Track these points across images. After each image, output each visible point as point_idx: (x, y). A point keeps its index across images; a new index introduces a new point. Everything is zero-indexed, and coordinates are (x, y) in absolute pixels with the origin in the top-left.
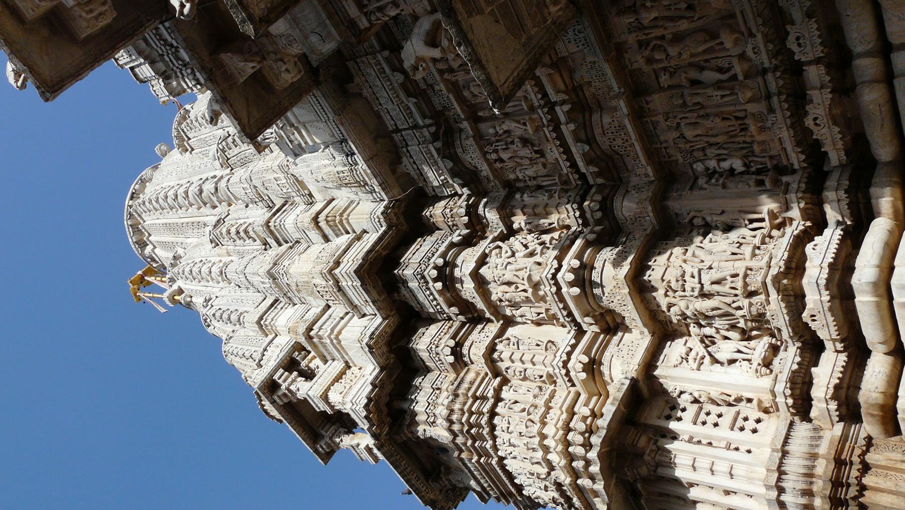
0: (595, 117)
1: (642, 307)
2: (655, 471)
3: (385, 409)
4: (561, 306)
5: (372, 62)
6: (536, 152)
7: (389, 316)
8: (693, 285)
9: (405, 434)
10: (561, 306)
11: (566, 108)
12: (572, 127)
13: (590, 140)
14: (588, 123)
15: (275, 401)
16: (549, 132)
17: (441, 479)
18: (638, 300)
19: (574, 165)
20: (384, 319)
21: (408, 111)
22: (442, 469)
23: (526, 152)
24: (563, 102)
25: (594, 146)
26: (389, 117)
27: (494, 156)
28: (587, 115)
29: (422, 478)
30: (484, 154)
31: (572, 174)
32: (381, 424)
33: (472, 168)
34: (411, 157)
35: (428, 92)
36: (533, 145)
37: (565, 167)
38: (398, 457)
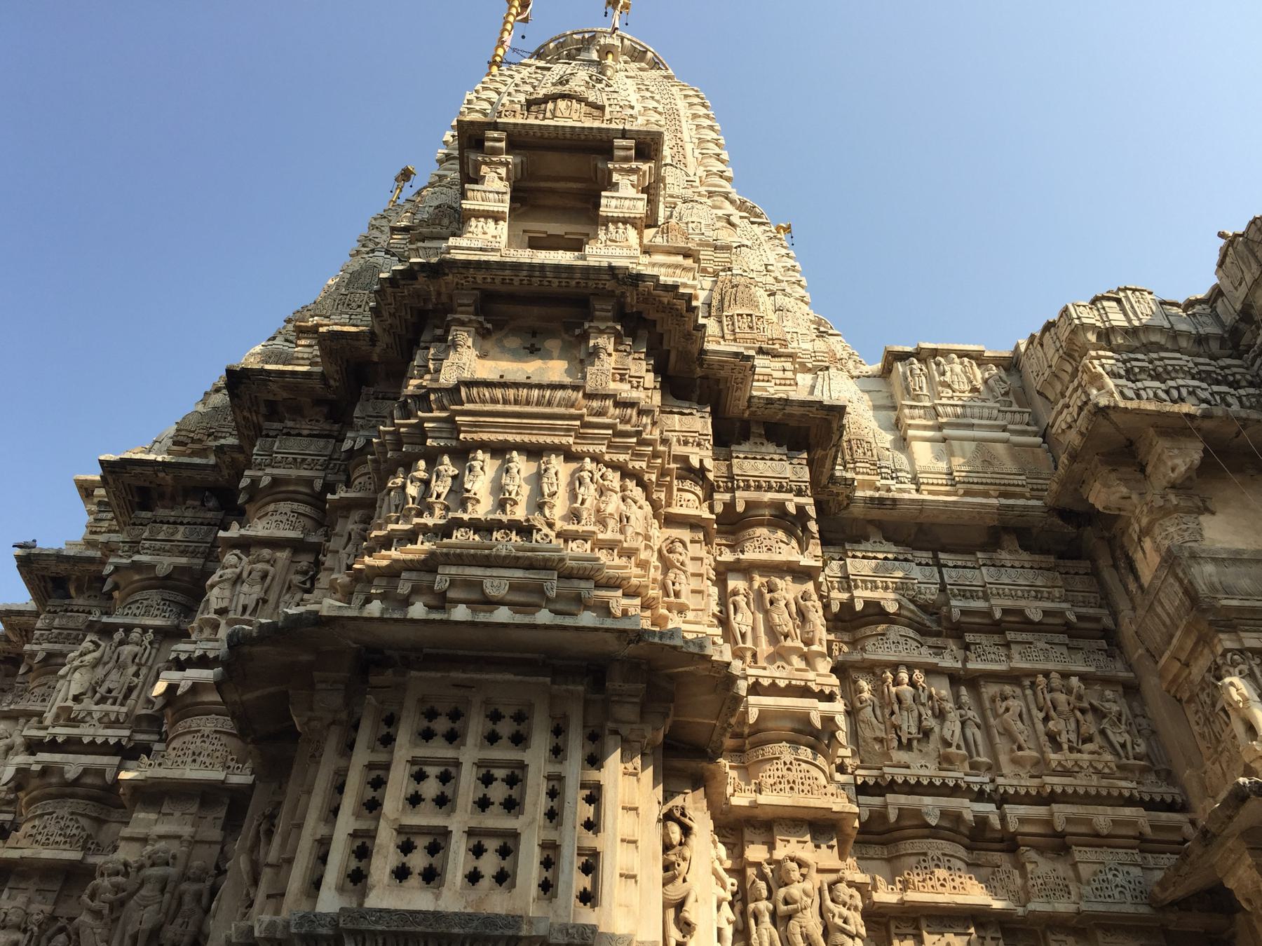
0: (962, 852)
1: (787, 814)
2: (616, 732)
3: (652, 315)
4: (782, 684)
5: (1056, 592)
6: (909, 740)
7: (749, 407)
8: (851, 921)
9: (604, 319)
10: (782, 684)
11: (995, 821)
12: (969, 816)
13: (934, 833)
14: (958, 837)
15: (624, 137)
16: (957, 779)
17: (476, 314)
18: (800, 814)
19: (892, 787)
20: (751, 397)
21: (968, 594)
22: (489, 326)
23: (909, 725)
24: (1003, 819)
25: (926, 831)
26: (959, 563)
27: (904, 676)
28: (967, 841)
29: (498, 286)
30: (910, 667)
31: (876, 777)
32: (648, 298)
33: (868, 631)
34: (896, 559)
35: (996, 637)
36: (919, 740)
37: (899, 775)
38: (573, 283)
